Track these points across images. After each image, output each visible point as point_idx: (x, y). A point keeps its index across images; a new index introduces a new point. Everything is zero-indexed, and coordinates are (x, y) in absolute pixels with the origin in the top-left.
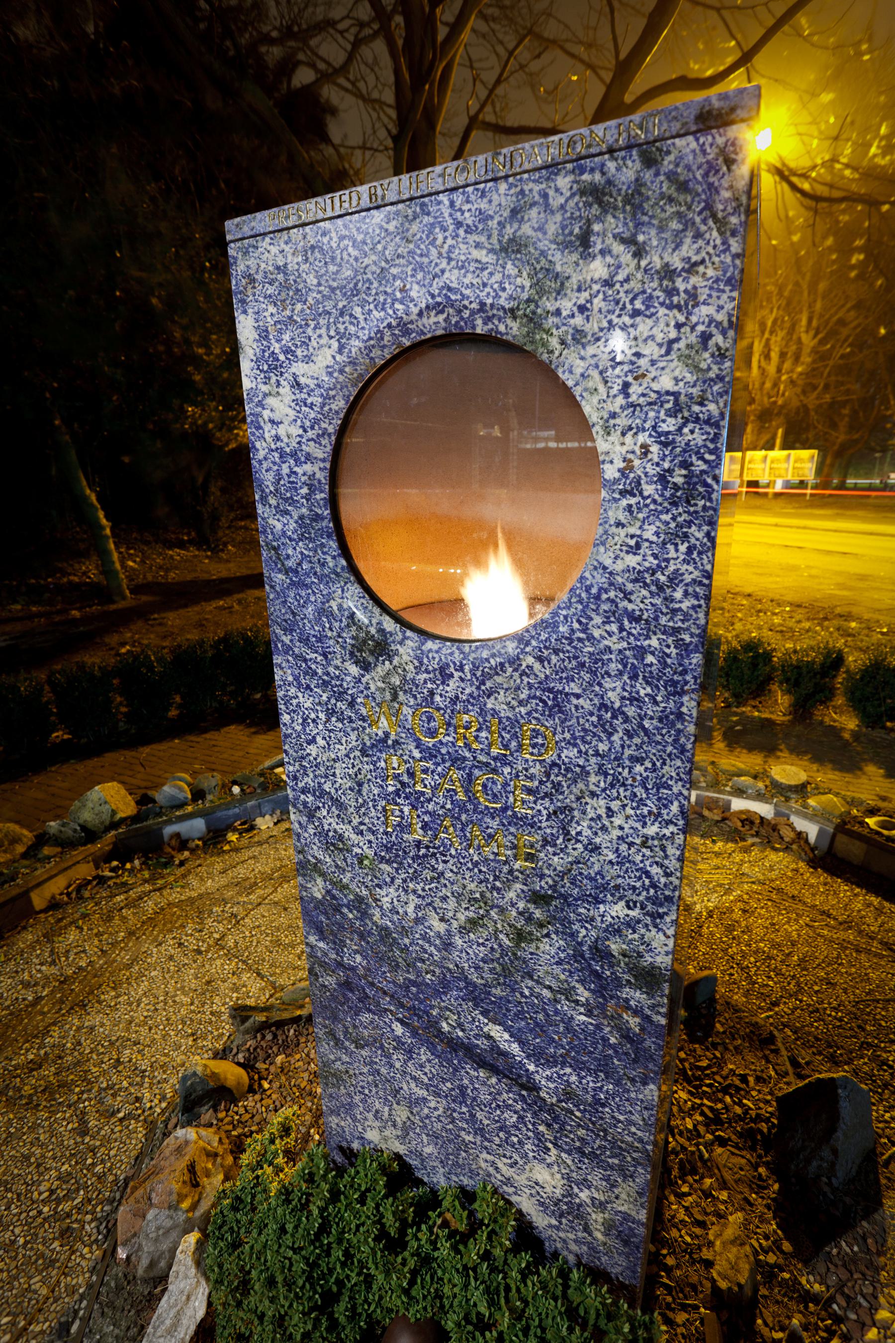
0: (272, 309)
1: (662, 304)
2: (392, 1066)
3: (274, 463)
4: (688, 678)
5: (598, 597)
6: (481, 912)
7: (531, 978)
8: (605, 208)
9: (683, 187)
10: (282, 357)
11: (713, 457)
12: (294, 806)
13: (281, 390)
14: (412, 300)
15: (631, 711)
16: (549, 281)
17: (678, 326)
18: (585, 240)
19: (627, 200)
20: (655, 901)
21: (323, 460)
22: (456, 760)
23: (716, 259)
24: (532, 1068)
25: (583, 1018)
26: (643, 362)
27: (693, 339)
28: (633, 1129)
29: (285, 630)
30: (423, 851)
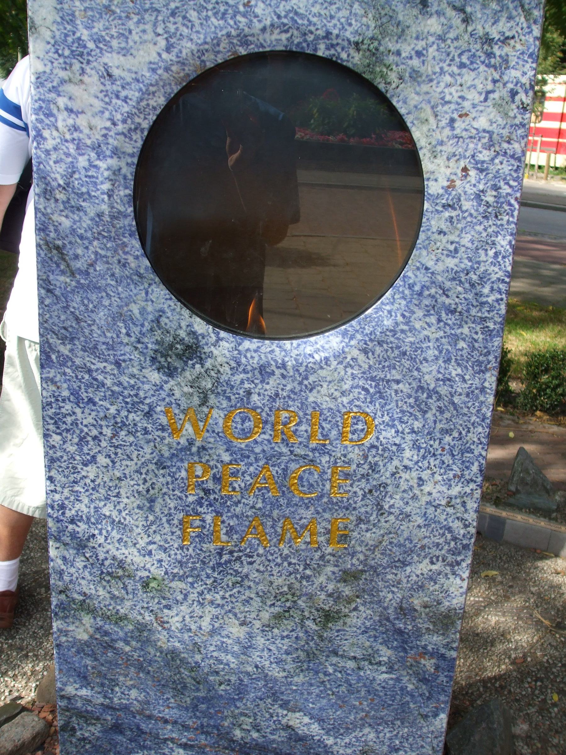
1: (483, 62)
3: (68, 155)
4: (491, 358)
5: (420, 294)
6: (288, 604)
7: (336, 654)
10: (91, 45)
11: (515, 184)
13: (86, 78)
14: (256, 16)
15: (444, 390)
17: (495, 81)
21: (132, 155)
23: (523, 38)
24: (330, 741)
25: (385, 676)
26: (467, 105)
27: (505, 93)
29: (63, 339)
30: (225, 557)
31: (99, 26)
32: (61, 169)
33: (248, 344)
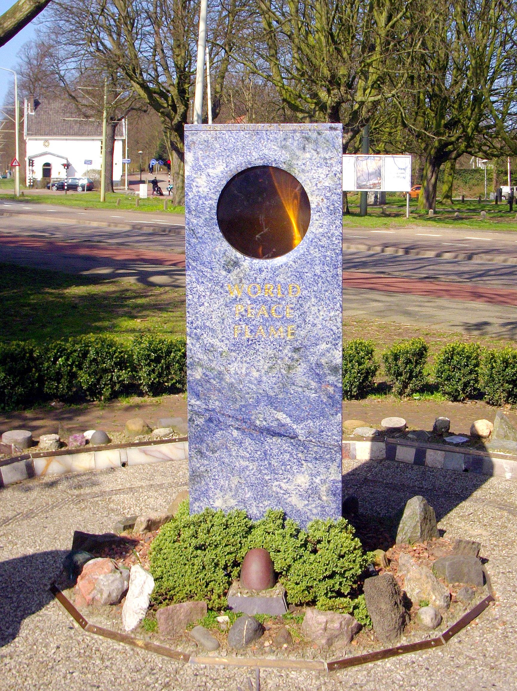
0: (201, 152)
2: (231, 455)
7: (294, 384)
8: (309, 142)
9: (328, 141)
10: (203, 167)
12: (190, 336)
15: (323, 275)
16: (293, 155)
18: (304, 148)
19: (314, 141)
20: (335, 340)
22: (265, 302)
24: (295, 427)
27: (333, 174)
28: (334, 437)
29: (194, 260)
30: (250, 342)
31: (206, 161)
32: (194, 204)
33: (256, 261)
